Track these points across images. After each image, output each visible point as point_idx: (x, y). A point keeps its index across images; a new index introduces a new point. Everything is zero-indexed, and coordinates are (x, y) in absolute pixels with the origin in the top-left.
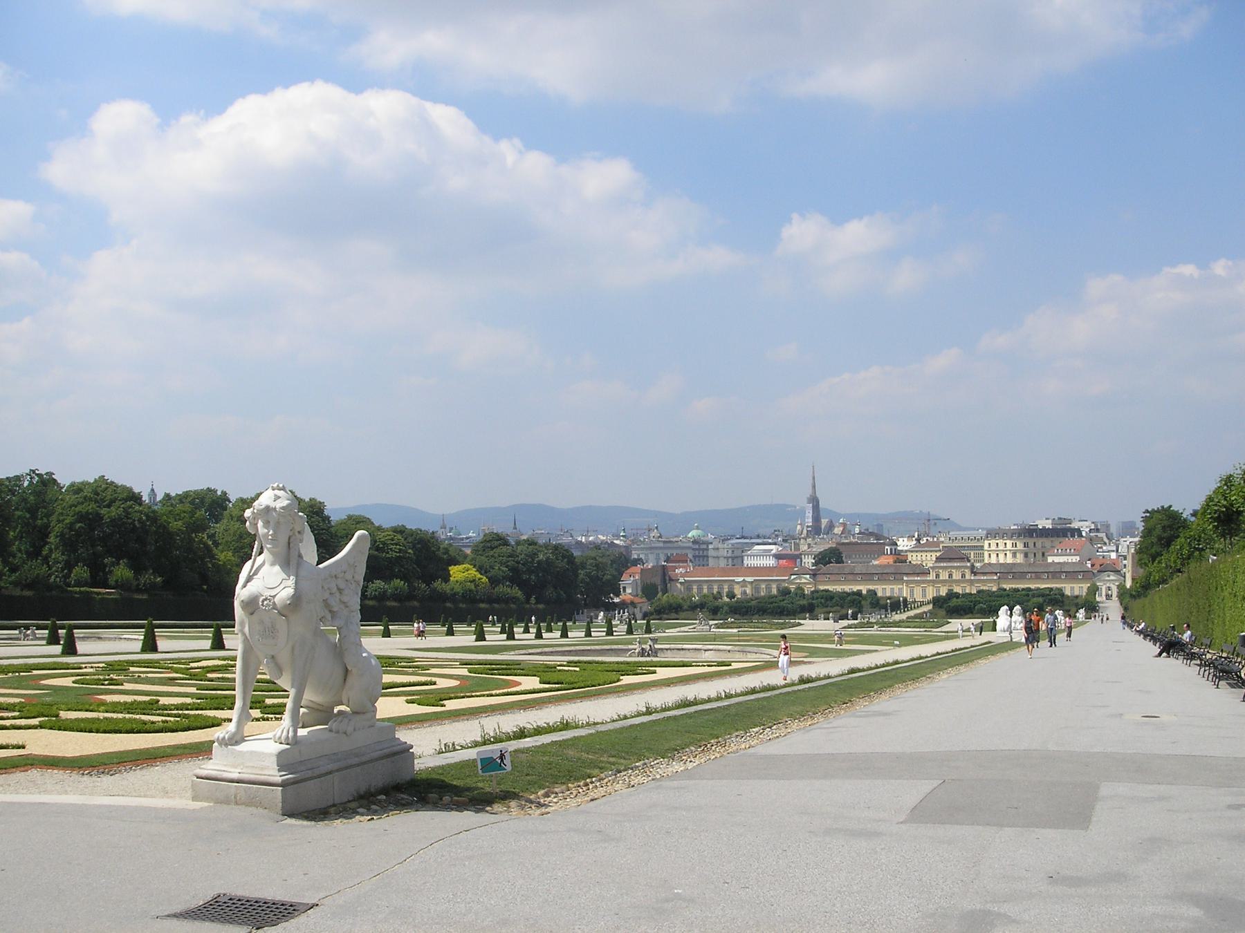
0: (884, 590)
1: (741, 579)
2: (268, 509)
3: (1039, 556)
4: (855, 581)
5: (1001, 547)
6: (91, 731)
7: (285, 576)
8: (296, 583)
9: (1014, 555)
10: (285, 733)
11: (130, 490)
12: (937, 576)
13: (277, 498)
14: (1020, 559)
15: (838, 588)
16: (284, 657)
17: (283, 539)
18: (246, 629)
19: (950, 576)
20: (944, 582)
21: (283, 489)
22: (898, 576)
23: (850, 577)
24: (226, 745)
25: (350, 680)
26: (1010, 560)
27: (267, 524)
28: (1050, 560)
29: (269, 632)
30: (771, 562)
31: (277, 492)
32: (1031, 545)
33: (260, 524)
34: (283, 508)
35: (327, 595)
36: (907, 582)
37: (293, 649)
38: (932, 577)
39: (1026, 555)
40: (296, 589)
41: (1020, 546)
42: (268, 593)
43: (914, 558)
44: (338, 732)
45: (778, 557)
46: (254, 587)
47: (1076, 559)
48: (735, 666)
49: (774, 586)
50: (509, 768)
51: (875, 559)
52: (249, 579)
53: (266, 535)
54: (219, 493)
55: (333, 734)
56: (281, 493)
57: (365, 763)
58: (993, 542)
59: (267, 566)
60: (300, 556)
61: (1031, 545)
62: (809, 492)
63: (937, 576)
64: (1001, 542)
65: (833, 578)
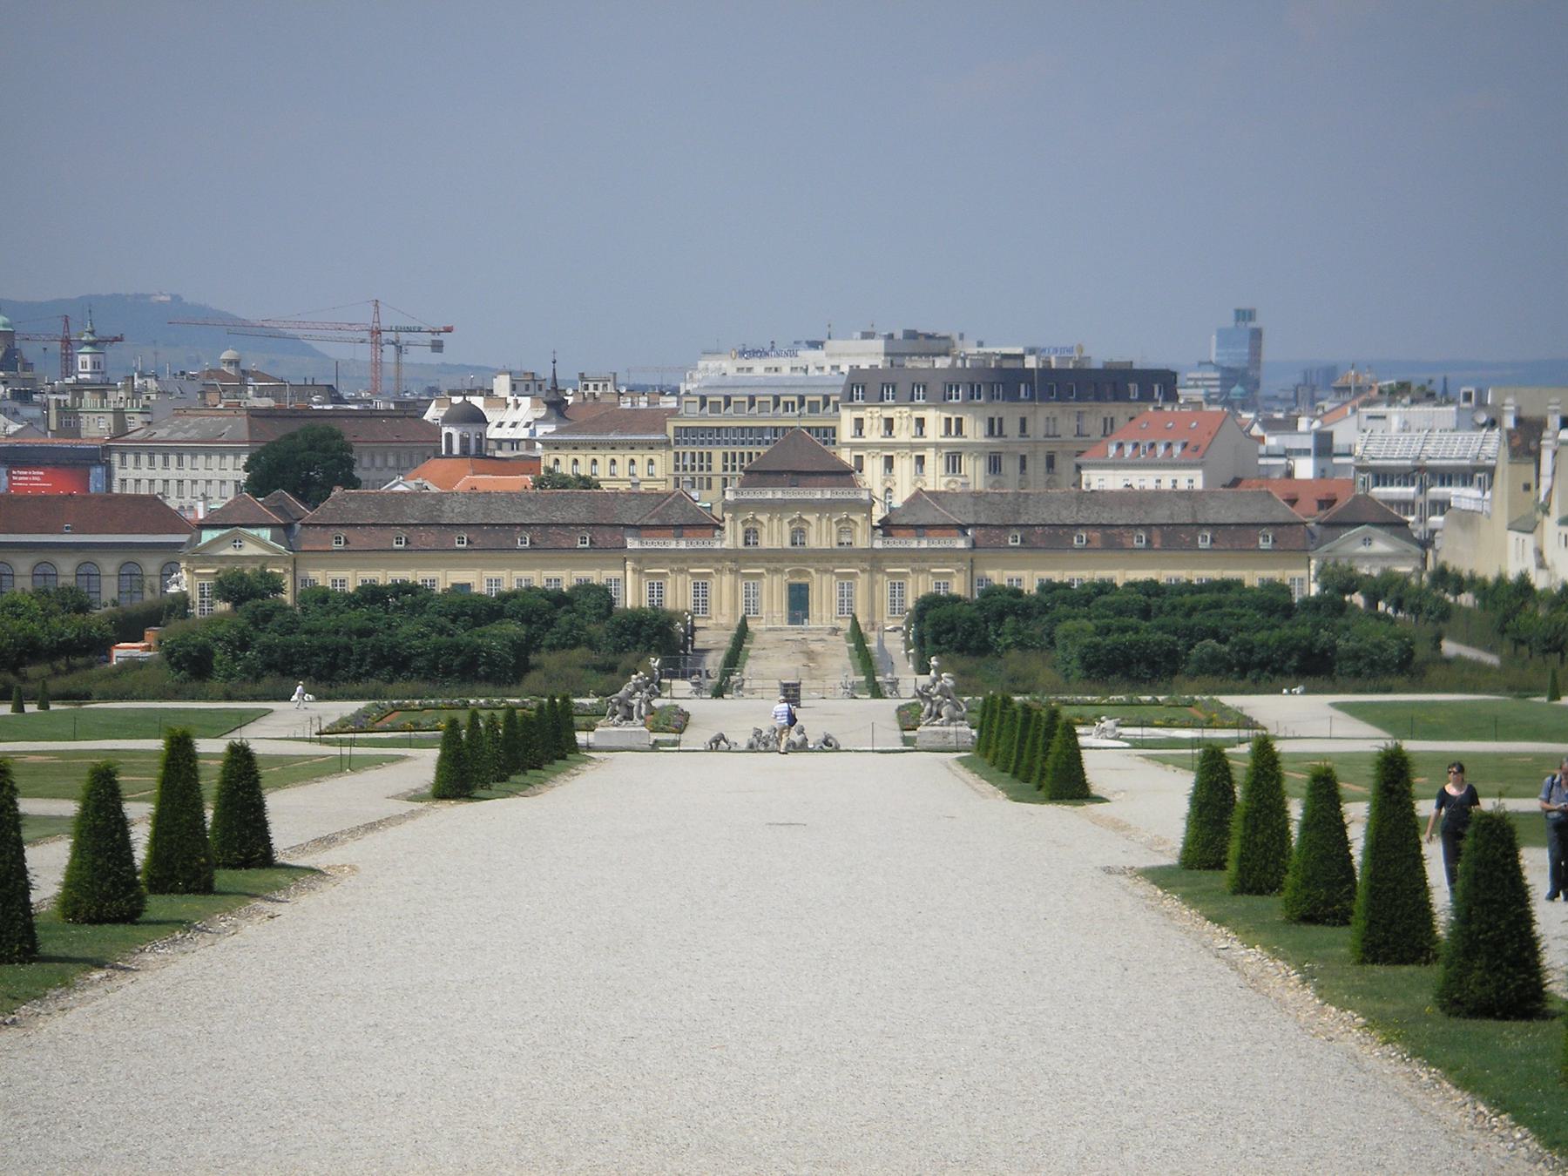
3: (1037, 467)
5: (904, 433)
12: (751, 534)
14: (974, 472)
15: (443, 578)
19: (798, 534)
20: (774, 558)
22: (605, 537)
23: (428, 538)
26: (936, 478)
32: (1012, 428)
36: (642, 557)
38: (731, 538)
39: (994, 464)
41: (974, 431)
47: (1192, 479)
49: (109, 566)
51: (401, 470)
58: (874, 417)
61: (1012, 428)
63: (751, 534)
64: (903, 416)
65: (360, 538)
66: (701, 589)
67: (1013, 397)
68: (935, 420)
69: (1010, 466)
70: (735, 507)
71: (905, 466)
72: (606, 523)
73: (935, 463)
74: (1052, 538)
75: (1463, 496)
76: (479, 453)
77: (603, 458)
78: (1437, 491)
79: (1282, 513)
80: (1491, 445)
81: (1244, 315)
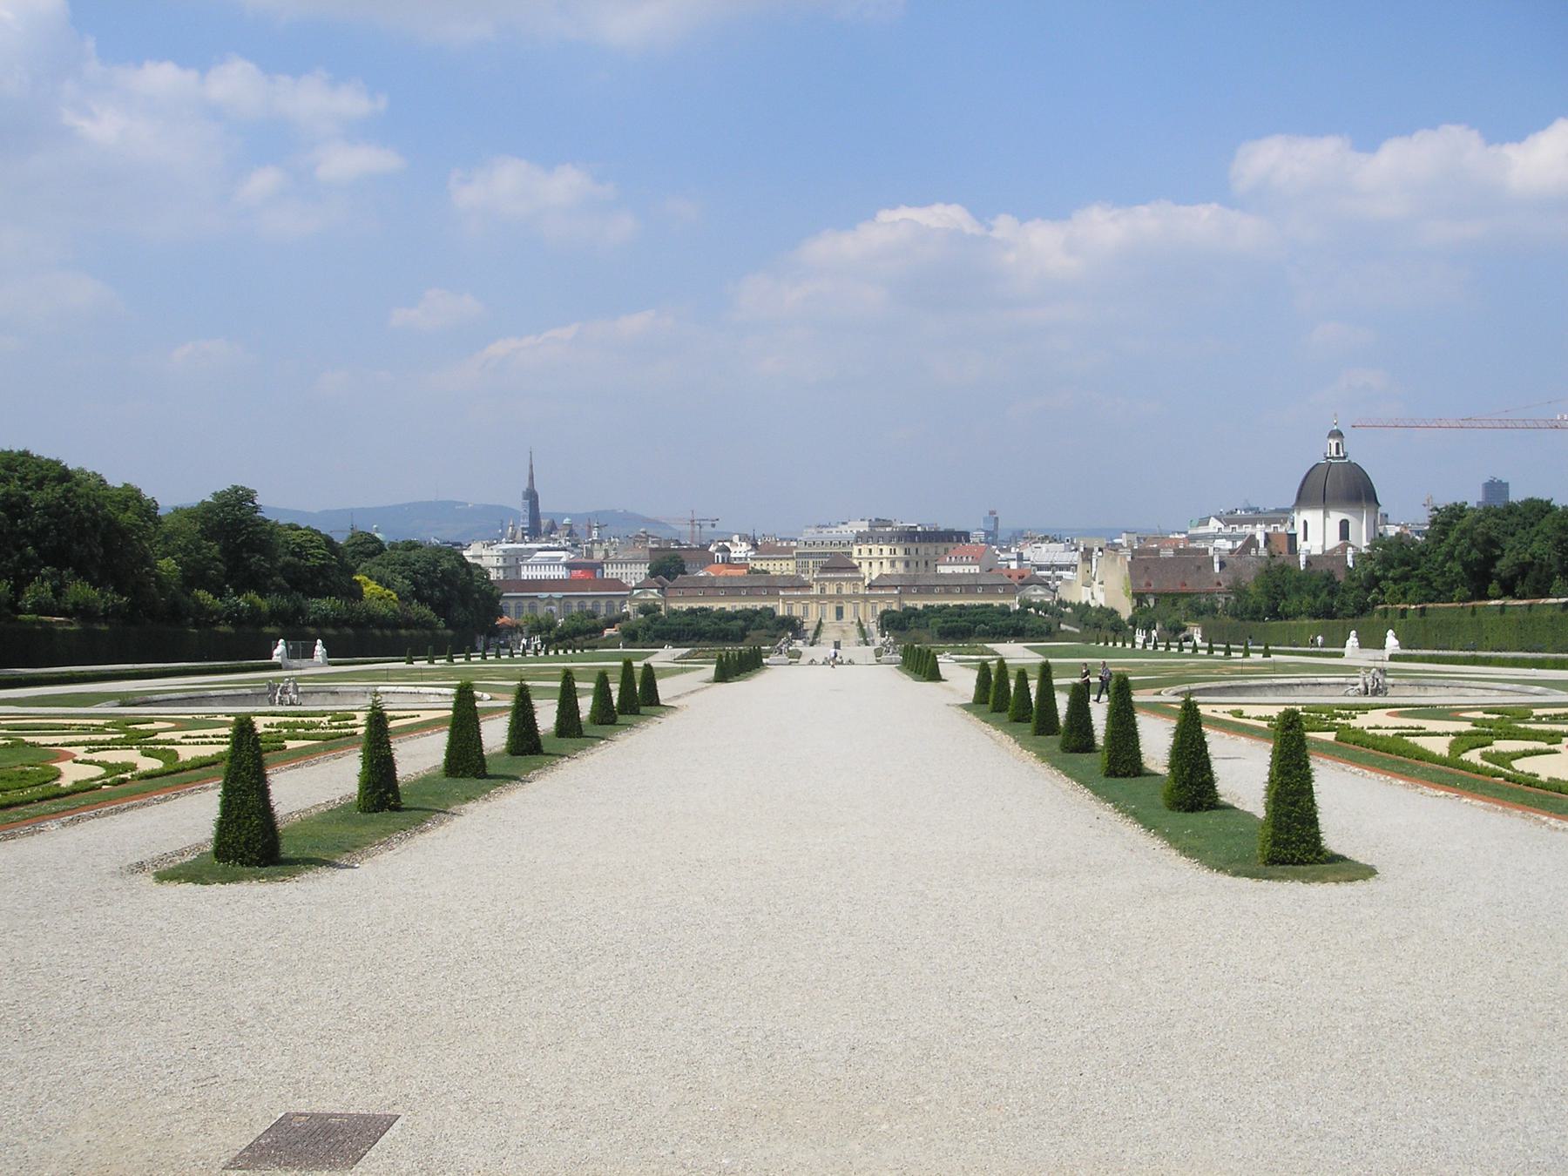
3: (922, 565)
4: (716, 597)
5: (875, 554)
9: (893, 564)
12: (823, 590)
14: (900, 567)
15: (716, 605)
19: (839, 589)
20: (831, 597)
23: (710, 591)
26: (887, 569)
30: (561, 573)
32: (913, 551)
36: (784, 597)
38: (816, 591)
39: (907, 564)
41: (900, 553)
45: (570, 566)
47: (975, 569)
49: (603, 603)
58: (865, 548)
61: (913, 551)
62: (526, 485)
63: (823, 590)
64: (875, 548)
65: (687, 592)
66: (806, 608)
68: (886, 549)
69: (913, 565)
71: (876, 565)
72: (772, 586)
73: (886, 564)
74: (927, 590)
75: (1067, 574)
76: (728, 562)
77: (771, 563)
78: (1058, 573)
79: (1006, 580)
80: (1075, 557)
81: (992, 513)
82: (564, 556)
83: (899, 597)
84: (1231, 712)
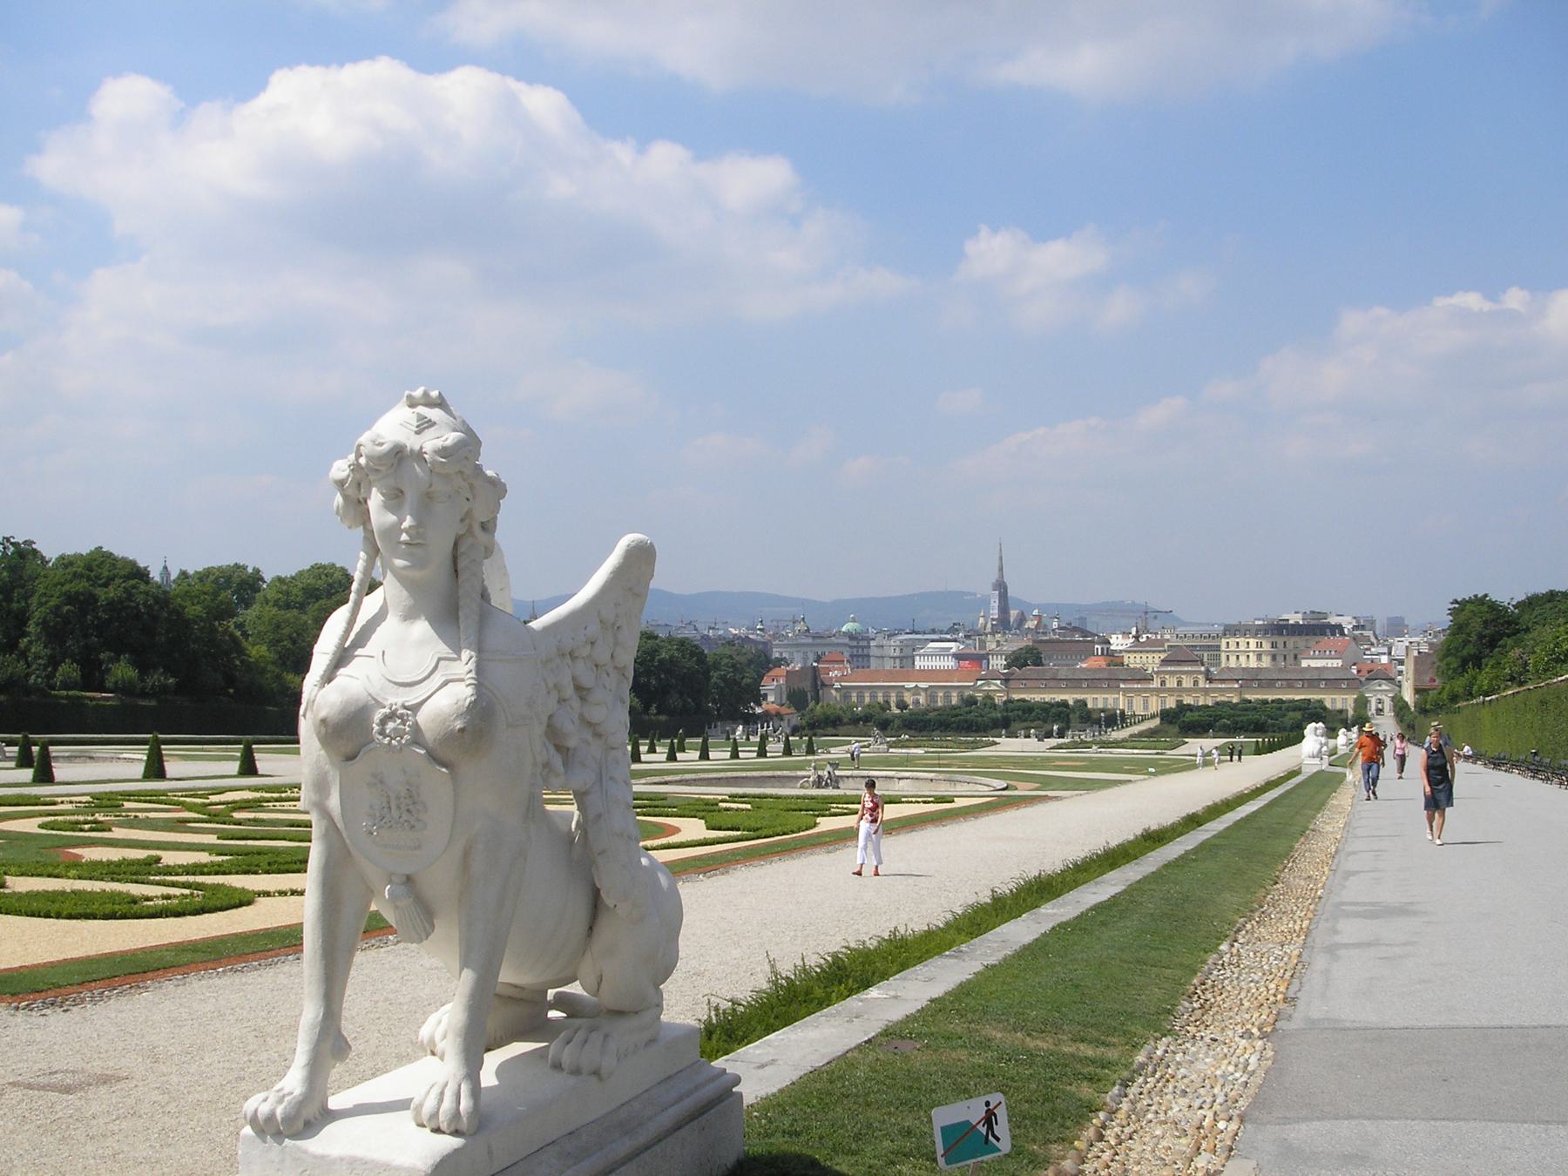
0: (1097, 700)
1: (912, 685)
2: (398, 455)
3: (1290, 659)
6: (48, 916)
7: (443, 649)
8: (480, 670)
9: (1259, 657)
10: (447, 1104)
11: (133, 564)
12: (1163, 683)
13: (425, 425)
14: (1266, 662)
15: (1037, 697)
16: (440, 880)
17: (440, 546)
18: (334, 802)
19: (1179, 683)
20: (1171, 690)
21: (441, 403)
22: (1112, 683)
23: (1052, 684)
24: (279, 1135)
25: (607, 931)
26: (1253, 663)
27: (395, 499)
28: (1304, 664)
29: (402, 809)
30: (950, 663)
31: (421, 410)
32: (1280, 645)
33: (375, 500)
34: (443, 452)
35: (552, 704)
37: (467, 854)
38: (1156, 684)
39: (1274, 658)
40: (479, 686)
41: (1266, 646)
42: (397, 699)
43: (1132, 661)
44: (576, 1072)
45: (958, 657)
46: (356, 681)
47: (1337, 663)
48: (960, 803)
49: (955, 694)
50: (1005, 1145)
51: (1082, 661)
52: (342, 658)
53: (392, 532)
54: (250, 570)
55: (562, 1080)
56: (435, 414)
57: (648, 1147)
58: (1232, 641)
59: (392, 623)
60: (484, 596)
61: (1280, 645)
62: (994, 576)
63: (1163, 683)
64: (1242, 641)
65: (1029, 684)
67: (1281, 634)
70: (1157, 673)
73: (1253, 657)
82: (954, 647)
83: (1240, 691)
84: (676, 830)
